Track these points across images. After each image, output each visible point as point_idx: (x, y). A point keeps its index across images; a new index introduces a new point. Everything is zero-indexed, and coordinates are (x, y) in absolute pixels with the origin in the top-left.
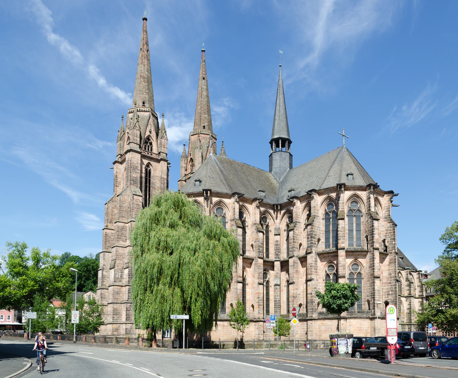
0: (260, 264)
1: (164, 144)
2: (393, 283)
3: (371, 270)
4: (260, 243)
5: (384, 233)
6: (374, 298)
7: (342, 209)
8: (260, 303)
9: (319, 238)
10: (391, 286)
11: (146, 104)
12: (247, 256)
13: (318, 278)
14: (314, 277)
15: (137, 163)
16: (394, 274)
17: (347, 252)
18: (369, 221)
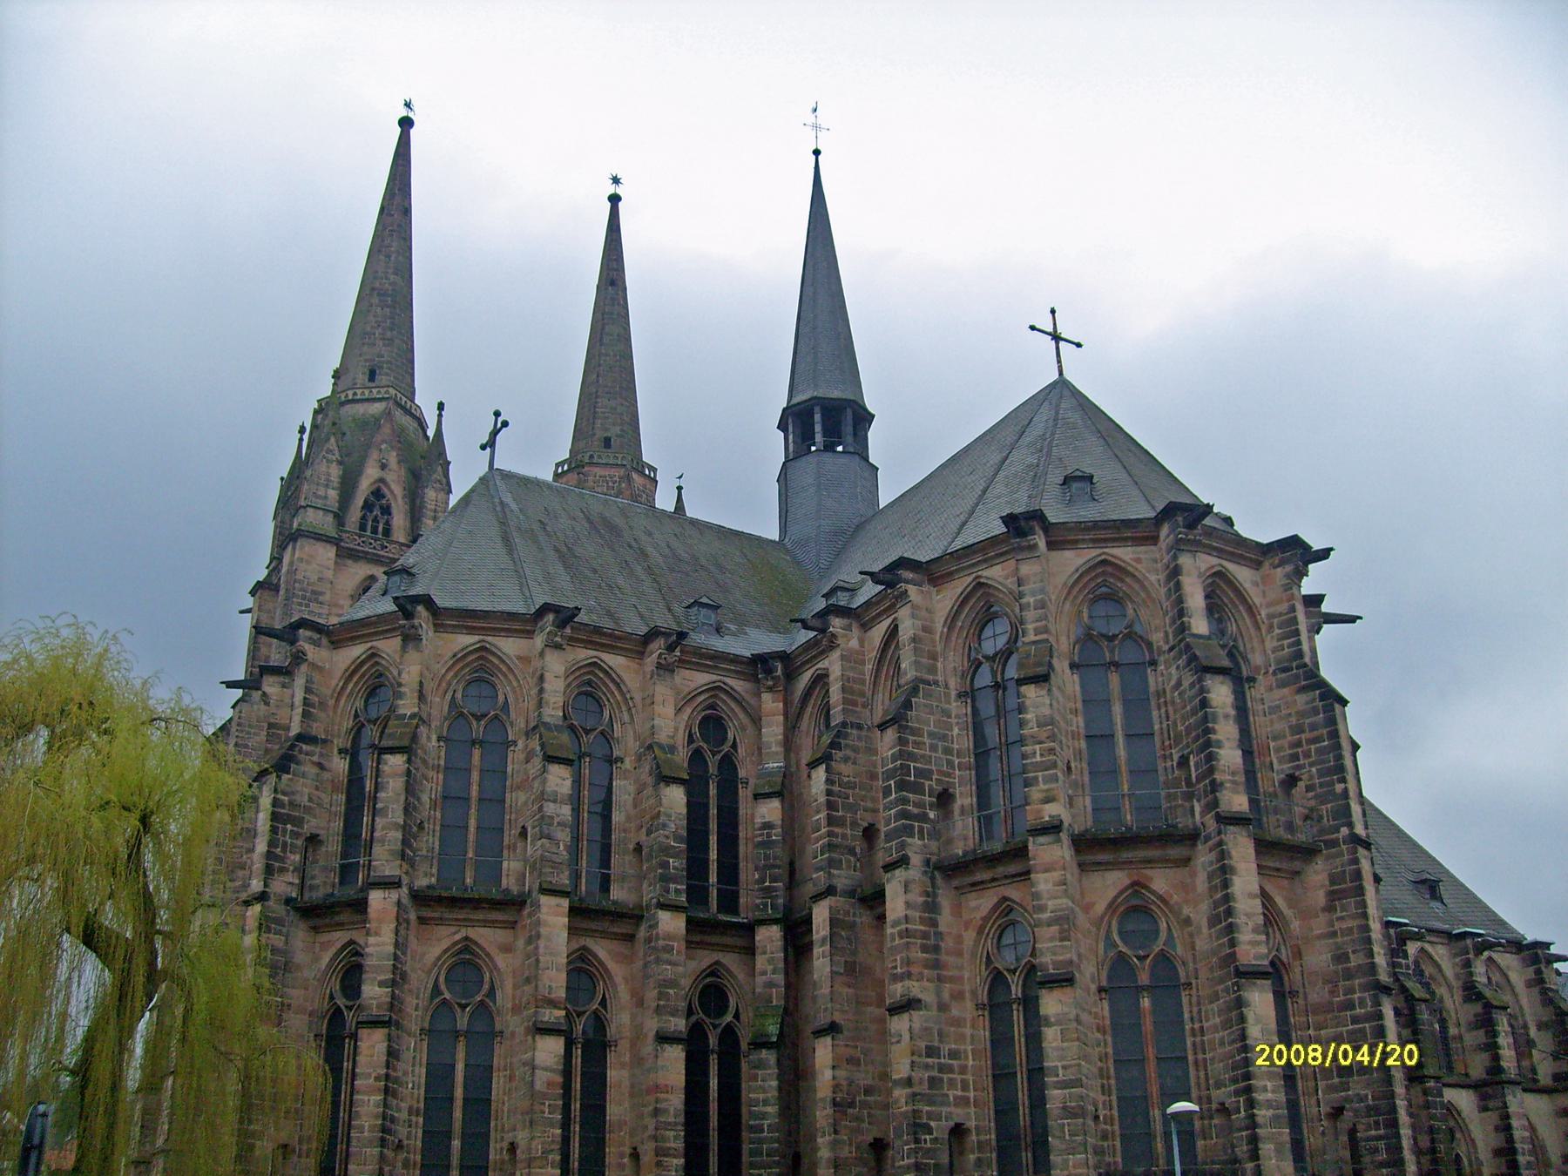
0: (669, 937)
1: (433, 507)
2: (1362, 1003)
3: (1218, 938)
4: (667, 837)
5: (1285, 743)
6: (1249, 1090)
7: (1037, 632)
8: (665, 1139)
9: (946, 790)
10: (1355, 1020)
11: (380, 374)
12: (615, 903)
13: (946, 996)
14: (924, 989)
15: (320, 579)
16: (1361, 954)
17: (1082, 843)
18: (1186, 684)
